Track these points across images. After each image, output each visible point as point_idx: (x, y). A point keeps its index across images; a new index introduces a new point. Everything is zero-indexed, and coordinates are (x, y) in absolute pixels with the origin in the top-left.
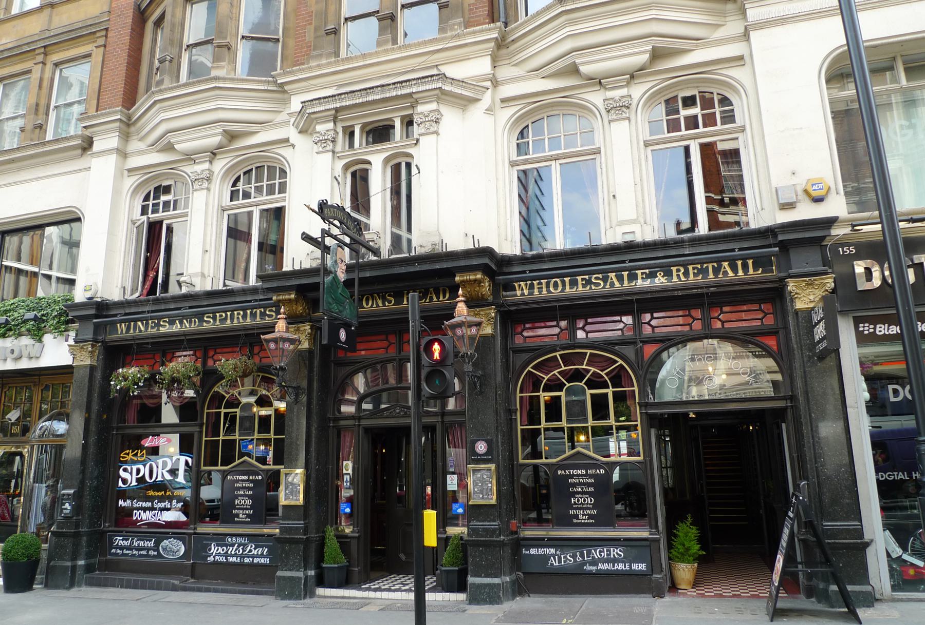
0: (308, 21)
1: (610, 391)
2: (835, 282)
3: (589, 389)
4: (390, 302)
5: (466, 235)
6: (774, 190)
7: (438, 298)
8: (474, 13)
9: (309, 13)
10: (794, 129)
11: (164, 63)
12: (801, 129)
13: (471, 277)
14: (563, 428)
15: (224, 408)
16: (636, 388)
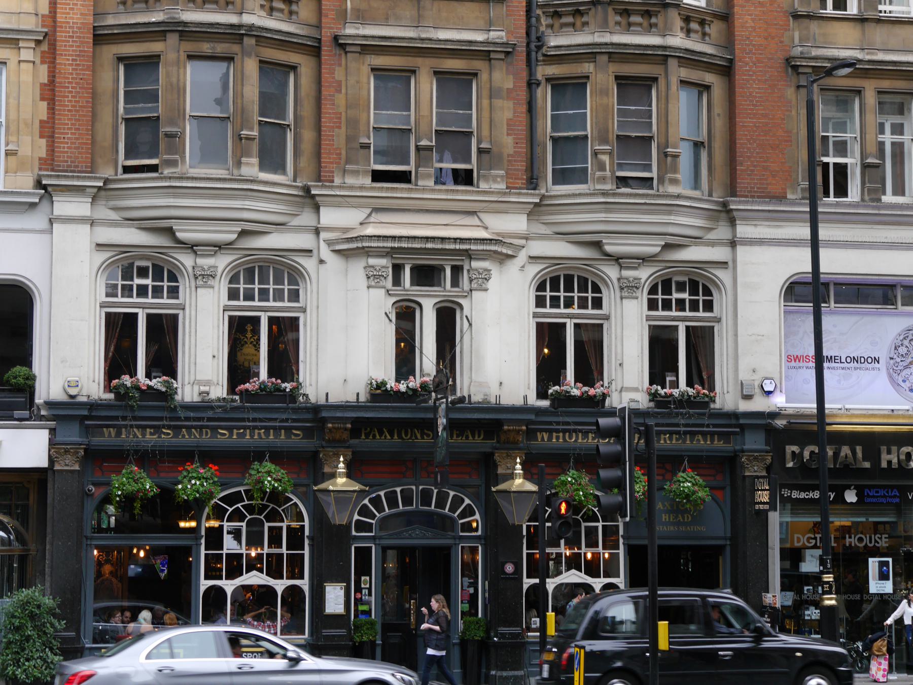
0: (334, 123)
1: (600, 525)
2: (772, 459)
3: (584, 522)
4: (428, 435)
5: (501, 383)
6: (740, 382)
7: (473, 437)
8: (512, 165)
11: (174, 139)
13: (517, 428)
15: (227, 521)
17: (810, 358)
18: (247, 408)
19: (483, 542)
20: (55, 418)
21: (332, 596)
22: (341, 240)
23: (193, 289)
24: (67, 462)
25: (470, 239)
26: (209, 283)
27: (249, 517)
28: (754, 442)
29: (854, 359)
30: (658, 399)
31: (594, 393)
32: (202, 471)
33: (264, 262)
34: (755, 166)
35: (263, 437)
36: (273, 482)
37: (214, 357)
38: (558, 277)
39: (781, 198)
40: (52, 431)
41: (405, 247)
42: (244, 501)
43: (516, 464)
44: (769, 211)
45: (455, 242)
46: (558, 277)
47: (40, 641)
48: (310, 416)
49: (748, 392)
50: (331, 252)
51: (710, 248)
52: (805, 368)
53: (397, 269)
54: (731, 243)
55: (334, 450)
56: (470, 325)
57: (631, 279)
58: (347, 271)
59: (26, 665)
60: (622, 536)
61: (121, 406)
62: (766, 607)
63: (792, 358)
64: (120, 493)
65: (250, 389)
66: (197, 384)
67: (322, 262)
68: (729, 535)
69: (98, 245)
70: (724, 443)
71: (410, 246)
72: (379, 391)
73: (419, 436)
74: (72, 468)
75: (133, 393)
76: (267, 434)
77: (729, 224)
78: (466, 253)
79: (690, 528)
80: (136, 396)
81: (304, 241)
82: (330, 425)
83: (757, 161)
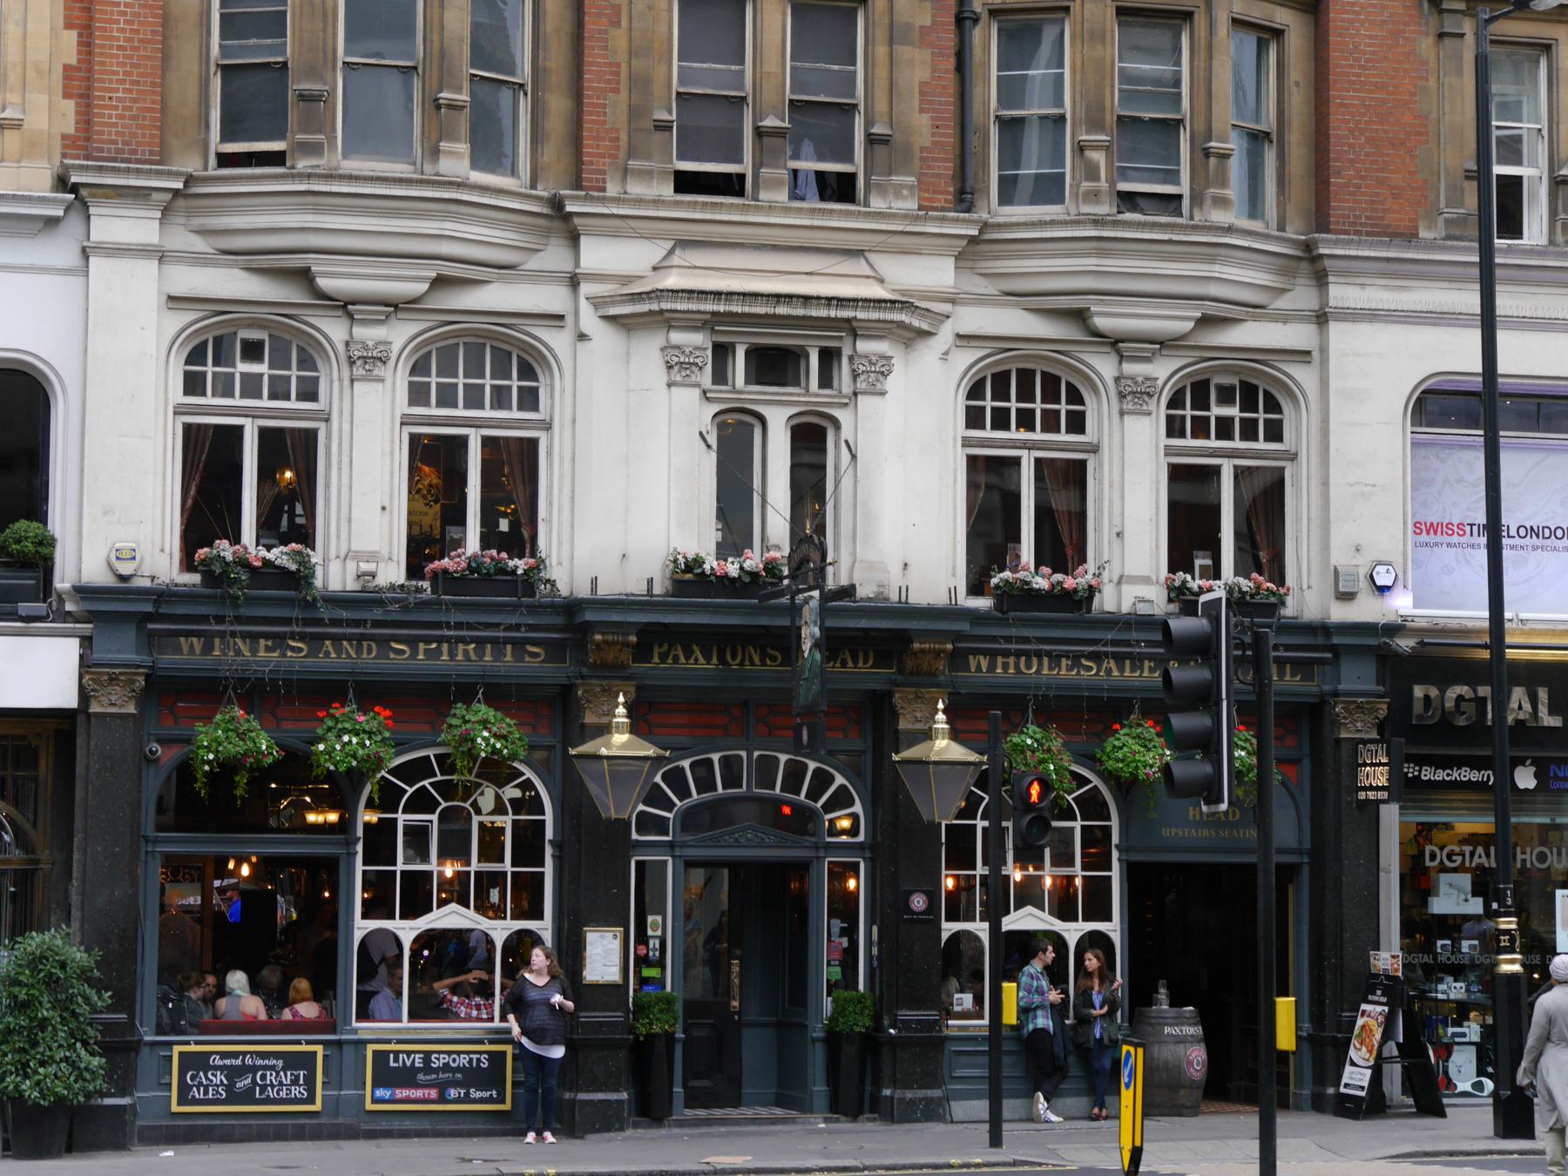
0: (608, 82)
1: (1077, 825)
2: (1388, 709)
4: (774, 659)
5: (906, 565)
6: (1332, 569)
7: (855, 662)
8: (928, 167)
9: (610, 64)
10: (1366, 485)
11: (317, 103)
12: (1374, 486)
13: (937, 646)
14: (506, 873)
15: (404, 812)
16: (1115, 823)
17: (1455, 528)
18: (446, 604)
19: (868, 855)
20: (91, 617)
21: (599, 950)
22: (620, 298)
23: (347, 383)
24: (113, 698)
25: (856, 300)
26: (375, 373)
27: (444, 805)
28: (1357, 678)
29: (1533, 531)
30: (1185, 598)
31: (1074, 586)
32: (363, 718)
33: (476, 336)
34: (1362, 178)
35: (473, 657)
36: (492, 740)
37: (384, 508)
38: (1008, 373)
39: (1409, 236)
40: (86, 641)
41: (737, 313)
42: (436, 776)
43: (937, 711)
44: (1388, 260)
45: (829, 305)
46: (1008, 373)
47: (66, 1028)
48: (559, 620)
49: (1346, 586)
50: (599, 320)
51: (1280, 325)
52: (1445, 545)
53: (722, 352)
54: (1317, 317)
55: (604, 683)
56: (854, 457)
57: (1140, 379)
58: (628, 353)
59: (40, 1074)
60: (1116, 846)
61: (214, 597)
62: (1377, 976)
63: (1423, 527)
64: (211, 756)
65: (451, 570)
66: (353, 558)
67: (582, 337)
68: (1307, 845)
69: (171, 298)
70: (1301, 680)
71: (747, 310)
72: (689, 576)
73: (756, 659)
74: (123, 711)
75: (238, 573)
76: (480, 652)
77: (1314, 283)
78: (845, 325)
79: (1239, 834)
80: (243, 578)
81: (550, 298)
82: (598, 637)
83: (1366, 169)
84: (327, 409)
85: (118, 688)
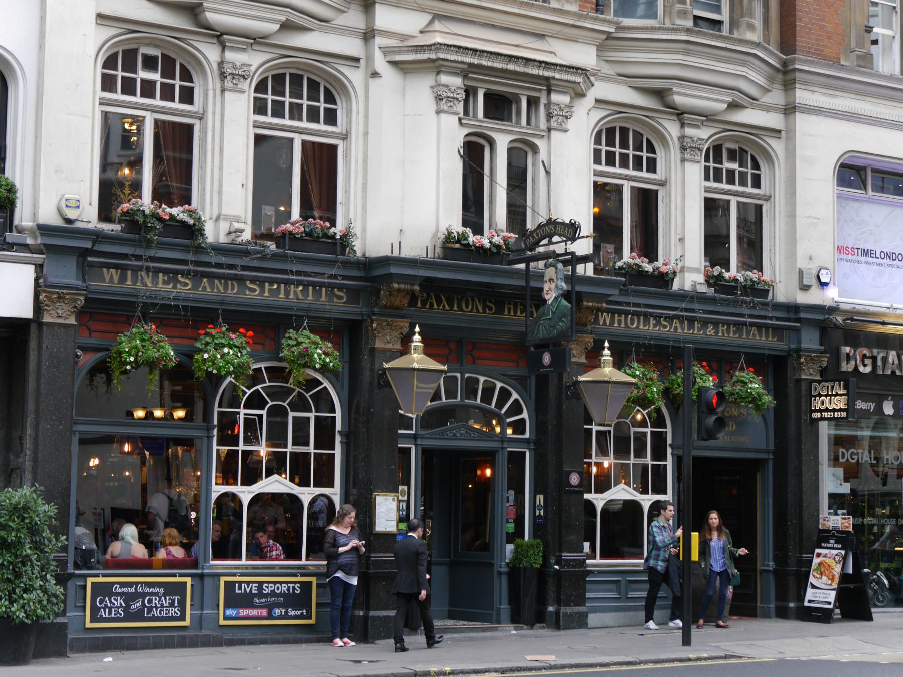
4: (490, 309)
6: (798, 270)
10: (815, 218)
12: (819, 219)
15: (245, 407)
17: (850, 250)
18: (291, 258)
19: (532, 446)
20: (49, 249)
21: (383, 509)
22: (406, 49)
23: (218, 92)
24: (60, 312)
25: (556, 65)
26: (239, 86)
27: (271, 403)
28: (810, 340)
29: (888, 256)
30: (721, 283)
31: (667, 270)
32: (233, 336)
33: (298, 69)
34: (812, 24)
35: (300, 297)
36: (323, 356)
37: (243, 185)
38: (613, 129)
39: (835, 62)
40: (39, 268)
41: (484, 65)
42: (266, 382)
43: (603, 348)
44: (829, 76)
45: (540, 66)
46: (613, 129)
47: (39, 563)
48: (361, 274)
49: (807, 281)
50: (386, 63)
51: (765, 112)
52: (845, 261)
53: (470, 92)
54: (785, 110)
55: (389, 320)
56: (548, 172)
57: (695, 139)
58: (404, 89)
59: (24, 599)
60: (670, 445)
61: (134, 240)
62: (829, 531)
64: (132, 359)
65: (294, 232)
66: (225, 219)
67: (375, 75)
68: (772, 447)
69: (100, 16)
70: (777, 341)
71: (490, 64)
72: (457, 246)
73: (480, 310)
74: (67, 322)
75: (153, 223)
76: (305, 292)
77: (782, 88)
78: (545, 82)
79: (735, 439)
80: (158, 227)
81: (351, 46)
82: (396, 286)
83: (815, 19)
84: (201, 111)
85: (64, 305)
